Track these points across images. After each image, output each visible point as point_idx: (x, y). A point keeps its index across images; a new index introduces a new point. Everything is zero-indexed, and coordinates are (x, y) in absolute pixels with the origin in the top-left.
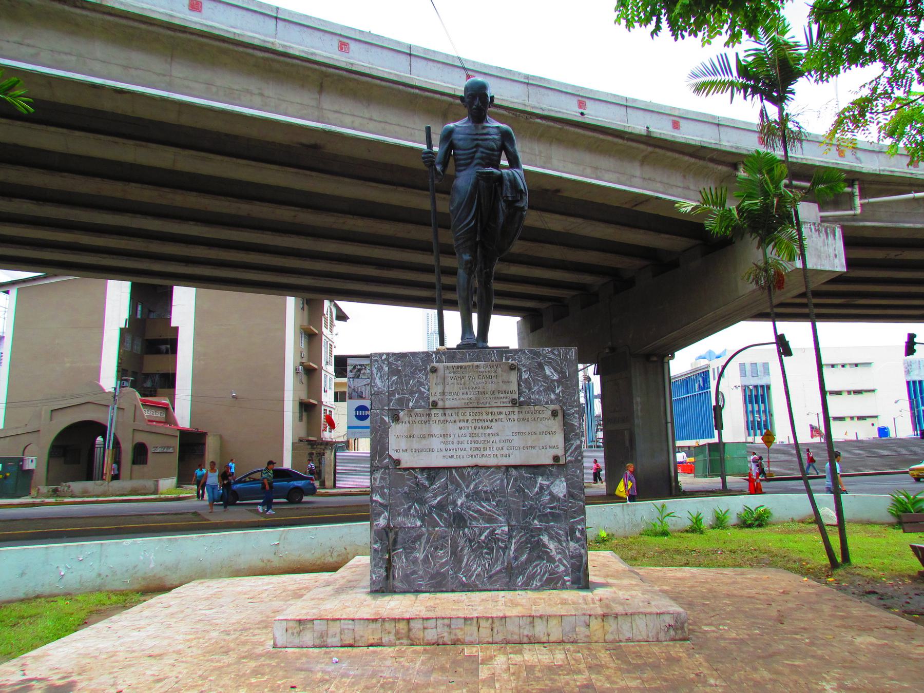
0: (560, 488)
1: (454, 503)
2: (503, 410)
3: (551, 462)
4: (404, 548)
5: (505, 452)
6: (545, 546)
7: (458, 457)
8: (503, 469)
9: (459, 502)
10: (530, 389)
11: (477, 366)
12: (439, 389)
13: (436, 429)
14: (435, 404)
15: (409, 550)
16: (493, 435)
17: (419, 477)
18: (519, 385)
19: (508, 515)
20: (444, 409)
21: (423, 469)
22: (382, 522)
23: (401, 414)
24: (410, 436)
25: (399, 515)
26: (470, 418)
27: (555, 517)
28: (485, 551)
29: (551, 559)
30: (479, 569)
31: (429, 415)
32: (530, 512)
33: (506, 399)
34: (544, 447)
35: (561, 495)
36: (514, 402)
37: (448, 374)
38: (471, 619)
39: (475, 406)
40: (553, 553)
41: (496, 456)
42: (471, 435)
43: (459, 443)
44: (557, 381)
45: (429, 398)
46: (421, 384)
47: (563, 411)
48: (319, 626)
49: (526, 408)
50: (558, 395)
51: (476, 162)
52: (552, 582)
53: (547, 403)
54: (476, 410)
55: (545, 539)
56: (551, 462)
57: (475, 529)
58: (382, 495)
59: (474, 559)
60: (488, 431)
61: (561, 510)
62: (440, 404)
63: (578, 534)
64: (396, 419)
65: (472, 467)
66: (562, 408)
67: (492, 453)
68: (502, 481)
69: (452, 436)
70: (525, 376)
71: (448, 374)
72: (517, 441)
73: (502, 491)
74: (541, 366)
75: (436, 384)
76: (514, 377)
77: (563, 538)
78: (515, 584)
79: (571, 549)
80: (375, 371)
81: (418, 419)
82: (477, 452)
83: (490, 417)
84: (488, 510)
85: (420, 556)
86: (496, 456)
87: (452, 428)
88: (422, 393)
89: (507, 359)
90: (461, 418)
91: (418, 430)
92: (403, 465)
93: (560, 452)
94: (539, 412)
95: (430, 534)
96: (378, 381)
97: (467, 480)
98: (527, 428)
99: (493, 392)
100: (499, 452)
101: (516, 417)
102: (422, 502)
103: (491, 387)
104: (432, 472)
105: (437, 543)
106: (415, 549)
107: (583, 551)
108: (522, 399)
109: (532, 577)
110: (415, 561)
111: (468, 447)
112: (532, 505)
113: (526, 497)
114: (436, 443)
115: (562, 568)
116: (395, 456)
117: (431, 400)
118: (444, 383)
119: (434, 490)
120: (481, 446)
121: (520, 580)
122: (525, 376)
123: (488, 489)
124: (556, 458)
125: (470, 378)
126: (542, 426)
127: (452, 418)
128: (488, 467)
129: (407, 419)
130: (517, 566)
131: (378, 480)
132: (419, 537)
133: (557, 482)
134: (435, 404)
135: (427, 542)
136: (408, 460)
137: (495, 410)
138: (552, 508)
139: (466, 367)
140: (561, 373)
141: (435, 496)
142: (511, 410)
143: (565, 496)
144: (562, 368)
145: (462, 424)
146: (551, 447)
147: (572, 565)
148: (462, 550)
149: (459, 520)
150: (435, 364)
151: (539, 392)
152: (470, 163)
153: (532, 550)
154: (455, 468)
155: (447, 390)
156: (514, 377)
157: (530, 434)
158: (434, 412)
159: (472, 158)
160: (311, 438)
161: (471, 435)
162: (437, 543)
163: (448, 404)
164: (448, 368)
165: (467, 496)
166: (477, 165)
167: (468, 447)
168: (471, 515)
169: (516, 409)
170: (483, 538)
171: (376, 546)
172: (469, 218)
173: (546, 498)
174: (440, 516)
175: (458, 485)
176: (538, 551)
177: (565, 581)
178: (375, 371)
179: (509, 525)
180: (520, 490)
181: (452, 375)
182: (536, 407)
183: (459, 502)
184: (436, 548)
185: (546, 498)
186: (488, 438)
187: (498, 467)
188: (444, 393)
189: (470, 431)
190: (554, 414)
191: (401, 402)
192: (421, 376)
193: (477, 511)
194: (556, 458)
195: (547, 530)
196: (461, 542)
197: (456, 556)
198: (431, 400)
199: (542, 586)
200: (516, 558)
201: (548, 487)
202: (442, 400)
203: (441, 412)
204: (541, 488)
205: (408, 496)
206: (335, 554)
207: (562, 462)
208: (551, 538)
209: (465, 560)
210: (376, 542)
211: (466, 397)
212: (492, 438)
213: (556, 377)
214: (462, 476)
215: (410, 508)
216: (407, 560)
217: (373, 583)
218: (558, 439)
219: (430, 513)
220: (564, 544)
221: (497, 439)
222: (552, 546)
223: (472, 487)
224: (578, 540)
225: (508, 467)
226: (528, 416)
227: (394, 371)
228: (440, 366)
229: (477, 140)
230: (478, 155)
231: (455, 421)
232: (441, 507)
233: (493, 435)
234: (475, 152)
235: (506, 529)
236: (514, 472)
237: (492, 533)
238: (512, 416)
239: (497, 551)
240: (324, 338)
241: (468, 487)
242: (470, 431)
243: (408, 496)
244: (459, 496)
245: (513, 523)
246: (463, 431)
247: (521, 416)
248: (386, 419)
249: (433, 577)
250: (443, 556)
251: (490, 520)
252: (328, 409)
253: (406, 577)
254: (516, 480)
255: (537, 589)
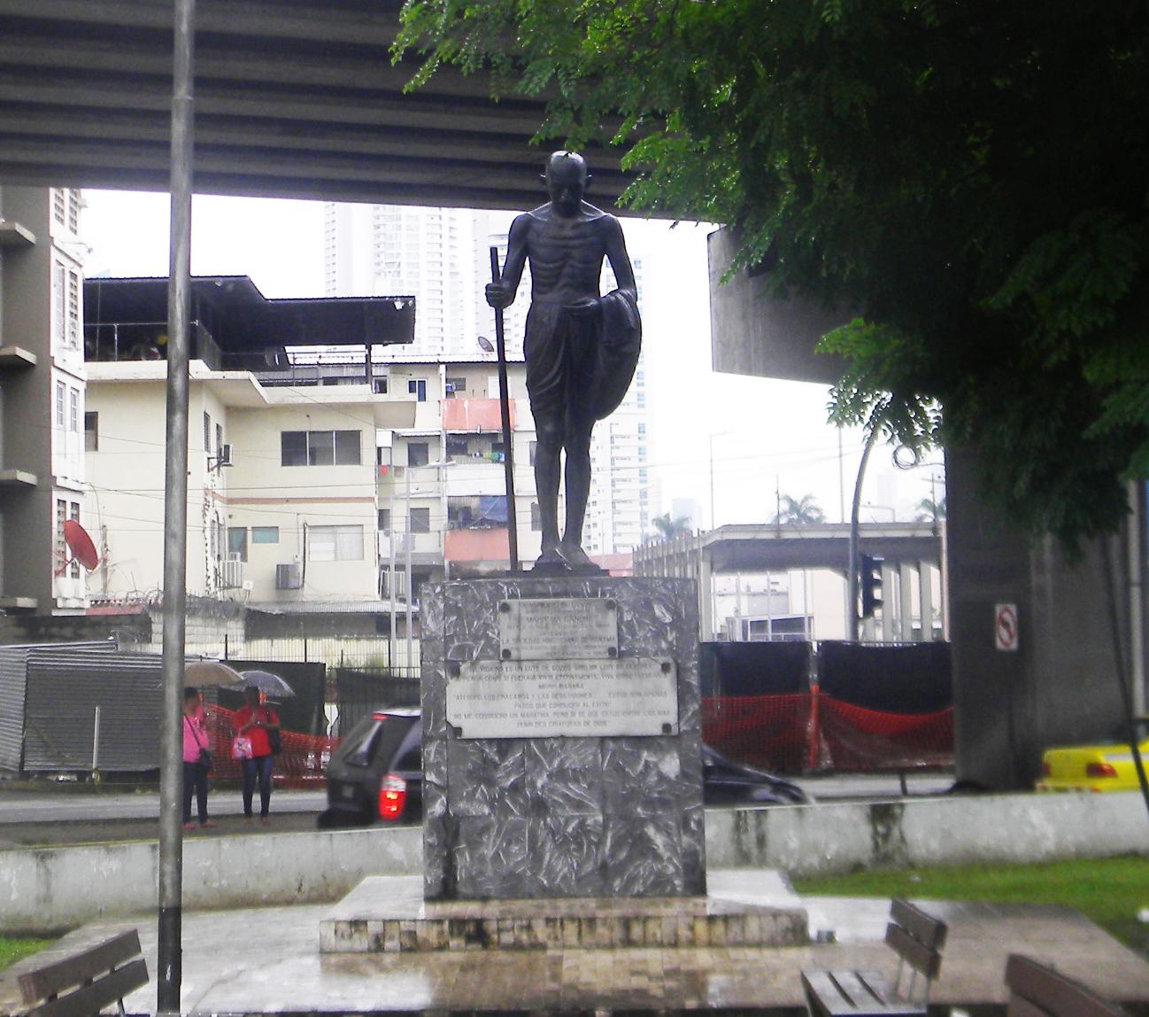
0: (671, 765)
1: (533, 784)
2: (596, 662)
3: (657, 731)
4: (469, 844)
5: (600, 717)
6: (649, 840)
7: (538, 723)
8: (597, 741)
9: (539, 783)
10: (633, 634)
11: (563, 603)
12: (513, 634)
13: (508, 686)
14: (507, 654)
15: (474, 845)
16: (584, 695)
17: (487, 750)
18: (619, 628)
19: (603, 799)
20: (519, 661)
21: (490, 741)
22: (437, 808)
23: (463, 668)
24: (475, 696)
25: (462, 799)
26: (554, 673)
27: (664, 803)
28: (573, 846)
29: (657, 857)
30: (566, 870)
31: (499, 669)
32: (632, 796)
33: (602, 647)
34: (651, 713)
35: (672, 776)
36: (612, 651)
37: (525, 615)
38: (554, 920)
39: (561, 658)
40: (661, 850)
41: (587, 723)
42: (556, 696)
43: (538, 706)
44: (671, 624)
45: (499, 646)
46: (487, 626)
47: (678, 664)
48: (374, 928)
49: (628, 660)
50: (670, 643)
51: (562, 282)
52: (659, 888)
53: (656, 654)
54: (561, 663)
55: (651, 831)
56: (657, 731)
57: (560, 818)
58: (439, 774)
59: (559, 857)
60: (578, 690)
61: (673, 794)
62: (514, 654)
63: (693, 825)
64: (455, 672)
65: (556, 738)
66: (675, 660)
67: (582, 720)
68: (595, 756)
69: (530, 697)
70: (627, 617)
71: (524, 614)
72: (616, 704)
73: (595, 769)
74: (648, 605)
75: (509, 627)
76: (611, 618)
77: (674, 831)
78: (611, 888)
79: (684, 845)
80: (426, 608)
81: (485, 673)
82: (562, 719)
83: (580, 672)
84: (577, 794)
85: (489, 852)
86: (587, 723)
87: (530, 686)
88: (489, 639)
89: (603, 594)
90: (542, 673)
91: (484, 687)
92: (466, 734)
93: (672, 718)
94: (645, 665)
95: (501, 824)
96: (429, 621)
97: (551, 754)
98: (628, 686)
99: (584, 639)
100: (591, 720)
101: (614, 671)
102: (491, 783)
103: (582, 631)
104: (504, 745)
105: (511, 836)
106: (481, 843)
107: (698, 848)
108: (623, 648)
109: (633, 880)
110: (482, 859)
111: (551, 711)
112: (633, 789)
113: (626, 776)
114: (508, 705)
115: (671, 869)
116: (455, 723)
117: (502, 648)
118: (519, 626)
119: (506, 767)
120: (569, 710)
121: (617, 884)
122: (627, 617)
123: (578, 766)
124: (666, 727)
125: (554, 619)
126: (649, 684)
127: (531, 673)
128: (576, 739)
129: (470, 674)
130: (614, 866)
131: (432, 755)
132: (486, 829)
133: (668, 758)
134: (507, 654)
135: (499, 831)
136: (472, 729)
137: (587, 663)
138: (660, 793)
139: (548, 605)
140: (675, 613)
141: (508, 775)
142: (608, 663)
143: (677, 777)
144: (676, 607)
145: (543, 681)
146: (659, 713)
147: (686, 866)
148: (544, 844)
149: (539, 807)
150: (507, 600)
151: (645, 639)
152: (555, 283)
153: (633, 846)
154: (536, 739)
155: (524, 634)
156: (611, 618)
157: (633, 694)
158: (506, 664)
159: (558, 276)
160: (24, 602)
161: (556, 696)
162: (511, 836)
163: (525, 654)
164: (525, 605)
165: (550, 776)
166: (565, 286)
167: (551, 711)
168: (554, 801)
169: (614, 663)
170: (570, 829)
171: (430, 840)
172: (551, 375)
173: (652, 779)
174: (515, 802)
175: (537, 761)
176: (643, 847)
177: (674, 887)
178: (426, 608)
179: (604, 814)
180: (619, 770)
181: (530, 615)
182: (642, 660)
183: (539, 783)
184: (509, 843)
185: (652, 779)
186: (577, 700)
187: (590, 739)
188: (518, 639)
189: (554, 690)
190: (665, 668)
191: (461, 650)
192: (487, 614)
193: (565, 796)
194: (666, 727)
195: (653, 820)
196: (542, 834)
197: (535, 853)
198: (502, 648)
199: (645, 891)
200: (613, 855)
201: (656, 765)
202: (518, 649)
203: (514, 665)
204: (647, 763)
205: (471, 775)
206: (305, 887)
207: (675, 731)
208: (658, 829)
209: (547, 858)
210: (432, 834)
211: (548, 645)
212: (581, 701)
213: (668, 619)
214: (543, 750)
215: (475, 790)
216: (471, 857)
217: (428, 886)
218: (669, 702)
219: (502, 796)
220: (675, 839)
221: (589, 701)
222: (659, 840)
223: (556, 763)
224: (693, 833)
225: (603, 739)
226: (631, 671)
227: (450, 609)
228: (514, 603)
229: (566, 247)
230: (567, 270)
231: (534, 677)
232: (516, 788)
233: (584, 695)
234: (563, 266)
235: (600, 818)
236: (611, 745)
237: (582, 824)
238: (609, 671)
239: (589, 847)
240: (54, 255)
241: (550, 763)
242: (554, 690)
243: (471, 775)
244: (540, 774)
245: (610, 811)
246: (544, 691)
247: (621, 671)
248: (443, 674)
249: (504, 879)
250: (519, 852)
251: (579, 805)
252: (69, 498)
253: (472, 880)
254: (613, 755)
255: (640, 895)
